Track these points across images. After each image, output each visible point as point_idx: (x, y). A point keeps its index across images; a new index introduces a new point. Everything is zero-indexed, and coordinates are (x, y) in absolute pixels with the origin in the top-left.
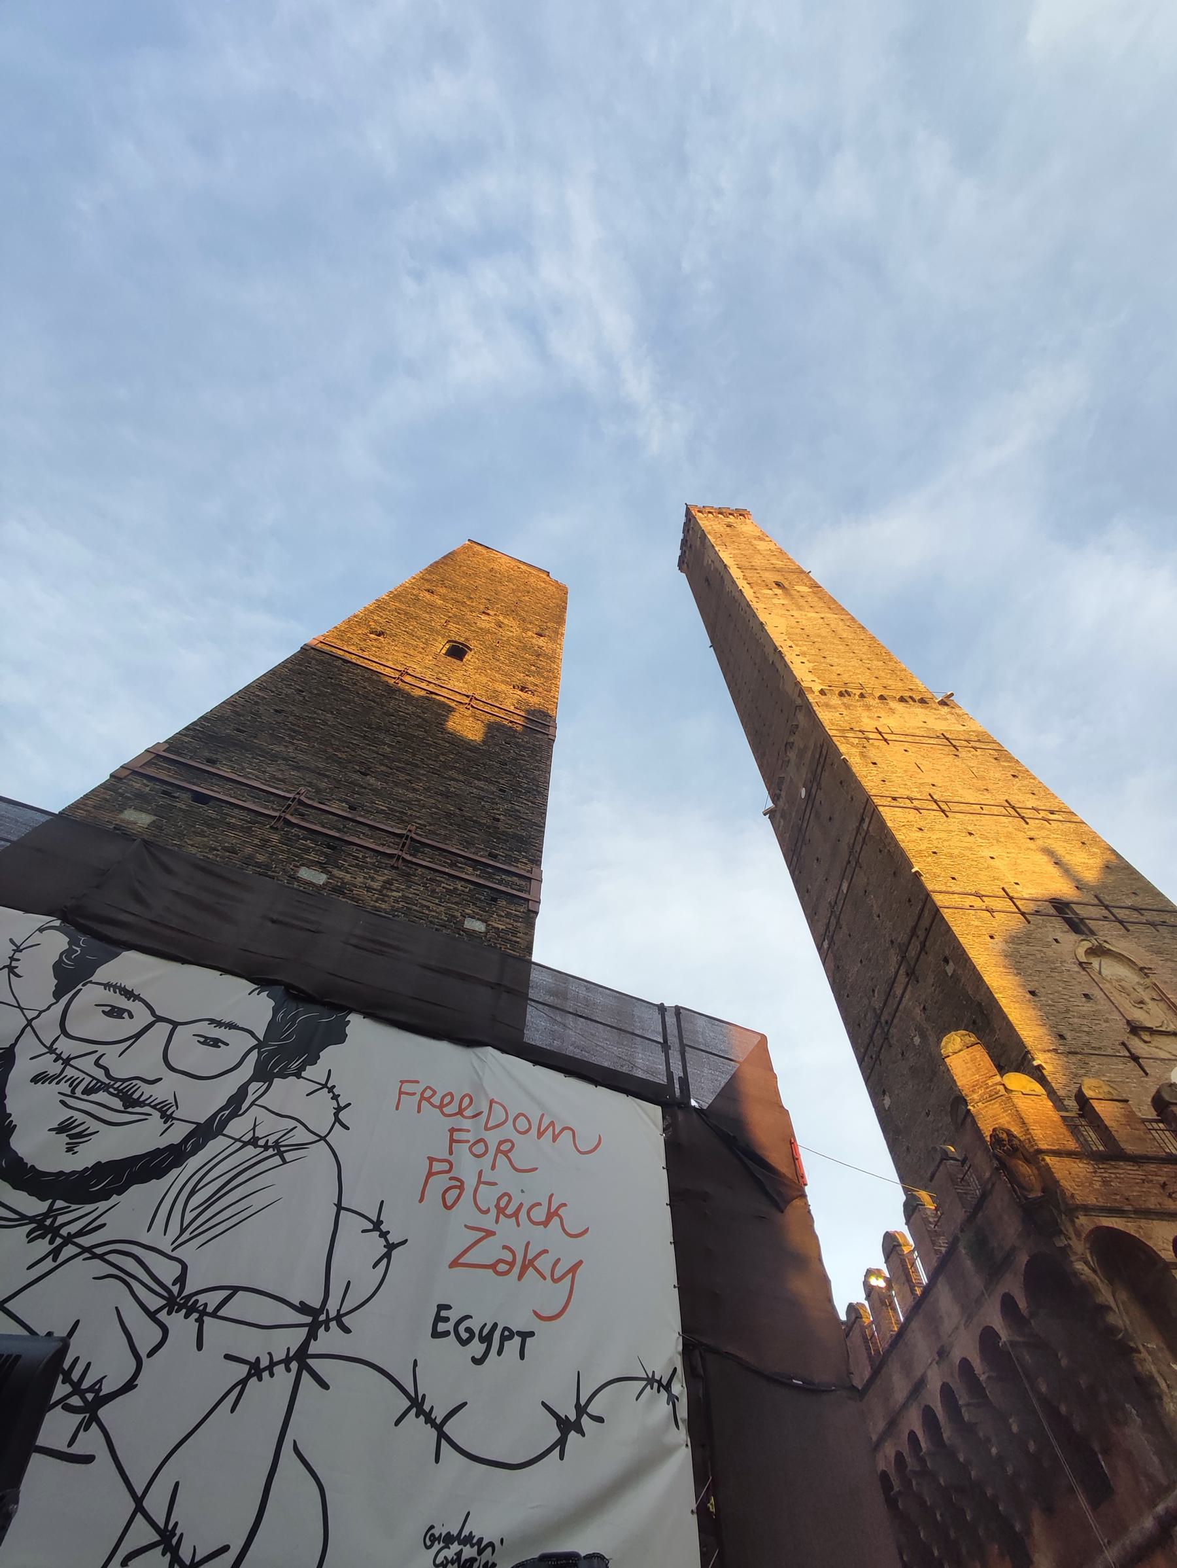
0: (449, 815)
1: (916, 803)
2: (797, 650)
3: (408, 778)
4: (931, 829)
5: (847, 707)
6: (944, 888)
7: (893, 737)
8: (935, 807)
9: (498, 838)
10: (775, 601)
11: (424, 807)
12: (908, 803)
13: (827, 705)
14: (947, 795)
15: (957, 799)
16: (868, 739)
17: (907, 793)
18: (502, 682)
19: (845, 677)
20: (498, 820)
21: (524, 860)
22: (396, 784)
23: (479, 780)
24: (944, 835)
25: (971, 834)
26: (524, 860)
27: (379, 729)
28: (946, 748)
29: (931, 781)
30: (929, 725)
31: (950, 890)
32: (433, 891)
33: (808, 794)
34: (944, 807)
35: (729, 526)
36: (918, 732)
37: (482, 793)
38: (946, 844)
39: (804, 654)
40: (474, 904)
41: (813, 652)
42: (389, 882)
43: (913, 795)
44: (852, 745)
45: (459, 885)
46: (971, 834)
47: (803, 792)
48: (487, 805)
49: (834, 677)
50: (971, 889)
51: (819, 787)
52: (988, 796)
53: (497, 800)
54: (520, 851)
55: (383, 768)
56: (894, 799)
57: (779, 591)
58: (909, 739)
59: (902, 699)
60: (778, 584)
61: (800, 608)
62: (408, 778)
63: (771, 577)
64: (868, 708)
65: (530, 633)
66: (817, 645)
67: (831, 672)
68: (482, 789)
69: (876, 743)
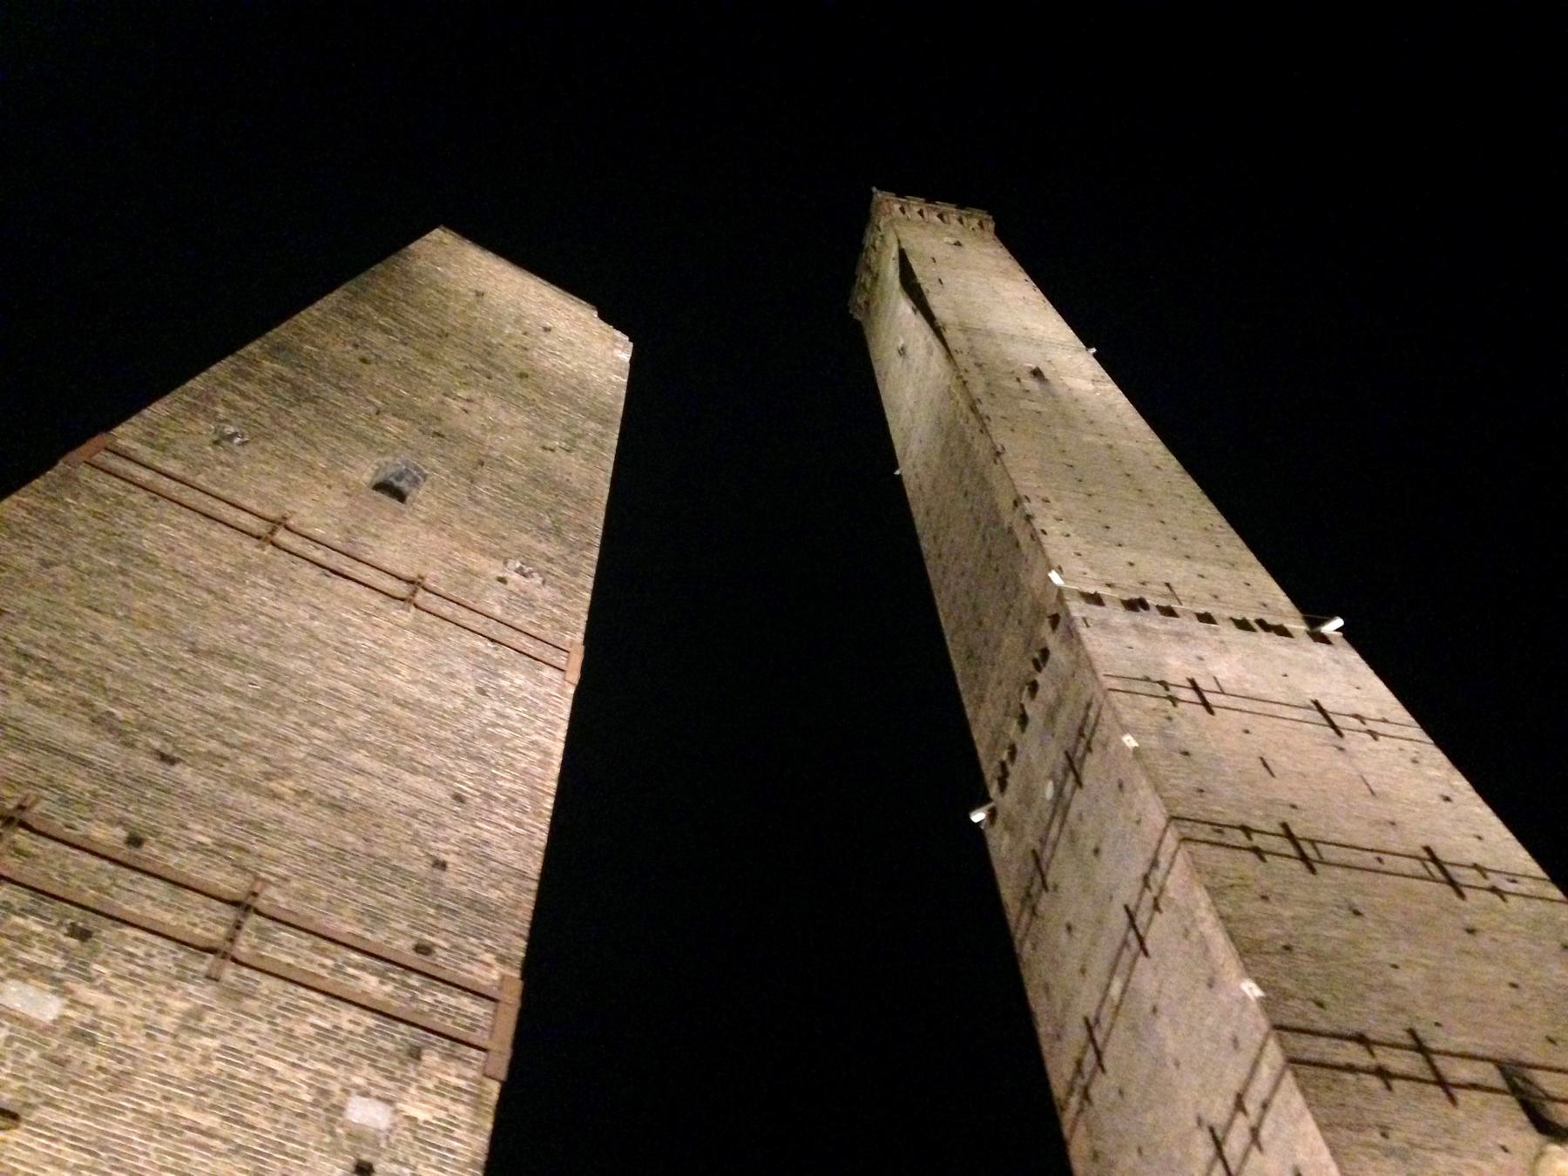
0: (341, 854)
1: (1257, 840)
3: (267, 768)
4: (1283, 898)
5: (1141, 630)
8: (1291, 850)
9: (439, 907)
11: (289, 835)
12: (1240, 838)
13: (1104, 625)
14: (1318, 830)
15: (1336, 837)
16: (1174, 700)
18: (483, 551)
20: (442, 865)
21: (488, 957)
22: (236, 782)
23: (414, 771)
24: (1304, 911)
25: (1357, 913)
26: (488, 957)
27: (211, 653)
32: (290, 1034)
33: (1059, 793)
34: (1309, 851)
37: (417, 804)
38: (1309, 930)
42: (197, 1014)
43: (1253, 823)
45: (346, 1017)
46: (1357, 913)
47: (1049, 791)
48: (425, 831)
50: (1354, 1027)
51: (1079, 782)
53: (446, 820)
55: (214, 745)
59: (1243, 625)
62: (267, 768)
68: (412, 792)
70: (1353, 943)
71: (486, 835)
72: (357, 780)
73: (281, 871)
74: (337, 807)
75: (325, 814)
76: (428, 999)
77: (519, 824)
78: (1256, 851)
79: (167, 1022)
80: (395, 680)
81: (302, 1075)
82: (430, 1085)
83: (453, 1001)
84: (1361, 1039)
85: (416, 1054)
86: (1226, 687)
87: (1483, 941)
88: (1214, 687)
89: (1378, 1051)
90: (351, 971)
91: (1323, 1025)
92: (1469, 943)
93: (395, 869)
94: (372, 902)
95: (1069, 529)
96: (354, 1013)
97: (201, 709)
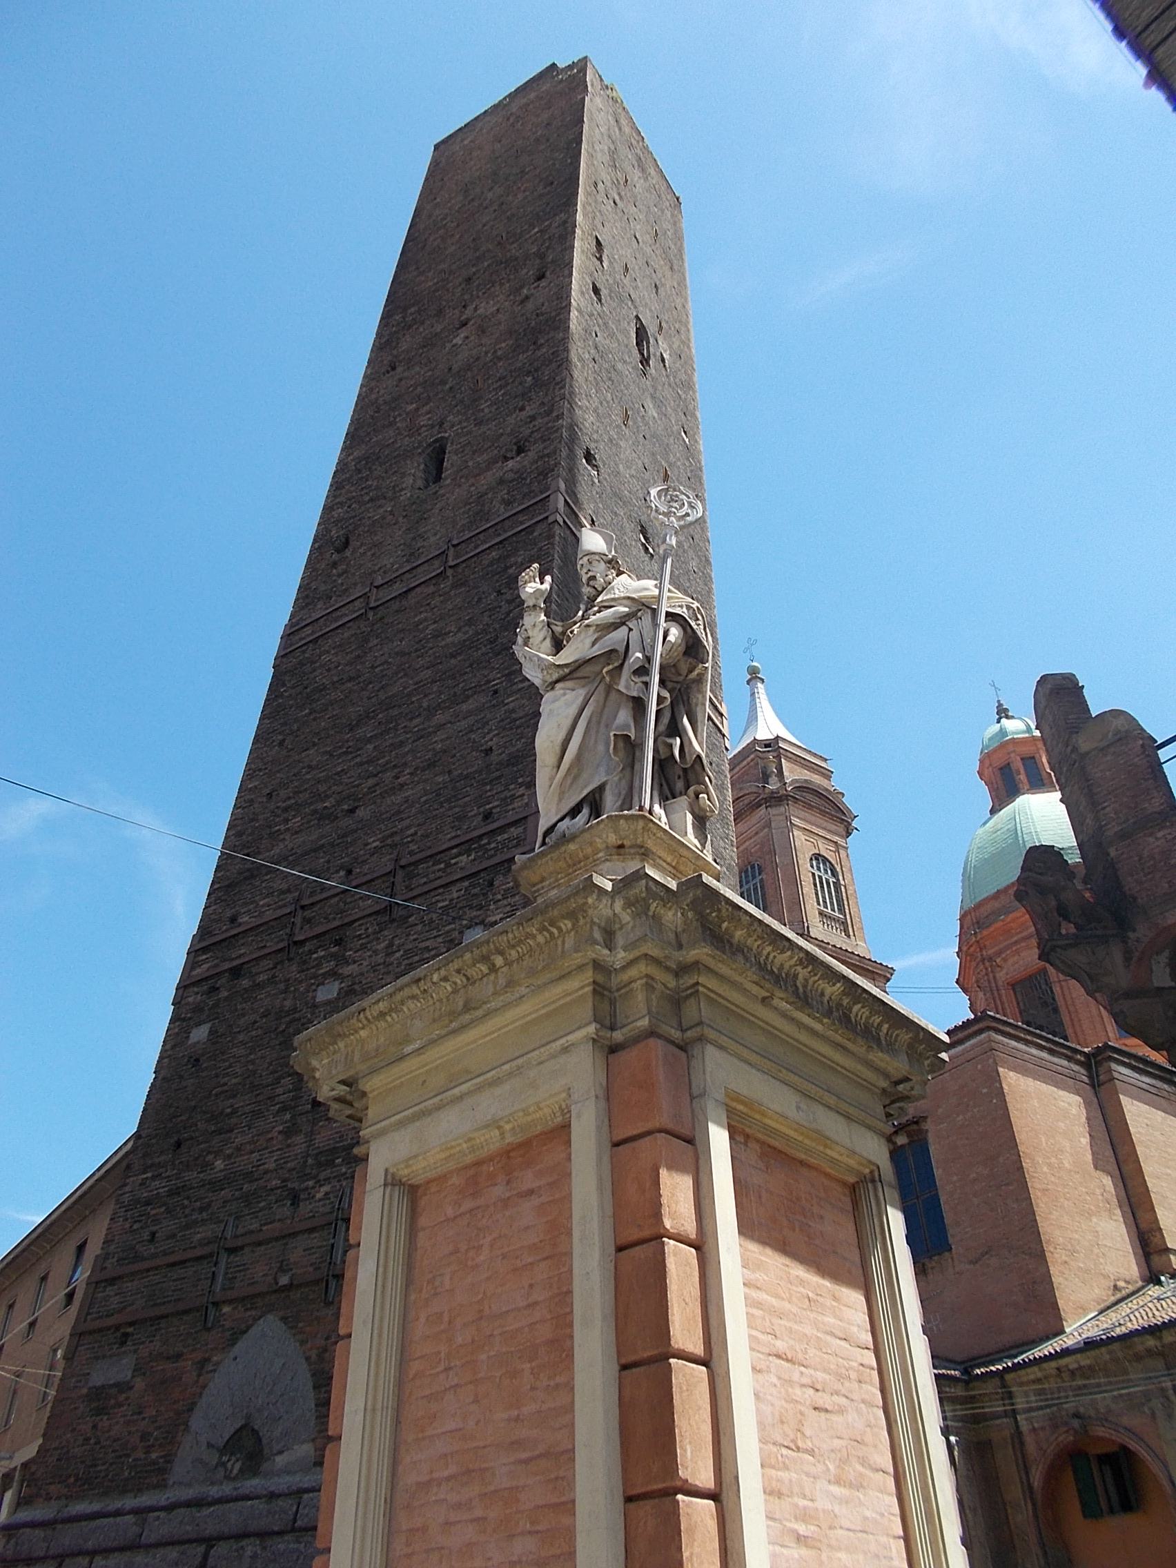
40: (471, 908)
42: (391, 945)
68: (470, 713)
72: (441, 735)
73: (412, 831)
74: (431, 765)
76: (493, 845)
79: (380, 958)
80: (449, 640)
81: (440, 940)
82: (499, 897)
83: (506, 836)
85: (491, 884)
90: (453, 861)
93: (467, 777)
94: (457, 810)
96: (458, 885)
97: (361, 764)
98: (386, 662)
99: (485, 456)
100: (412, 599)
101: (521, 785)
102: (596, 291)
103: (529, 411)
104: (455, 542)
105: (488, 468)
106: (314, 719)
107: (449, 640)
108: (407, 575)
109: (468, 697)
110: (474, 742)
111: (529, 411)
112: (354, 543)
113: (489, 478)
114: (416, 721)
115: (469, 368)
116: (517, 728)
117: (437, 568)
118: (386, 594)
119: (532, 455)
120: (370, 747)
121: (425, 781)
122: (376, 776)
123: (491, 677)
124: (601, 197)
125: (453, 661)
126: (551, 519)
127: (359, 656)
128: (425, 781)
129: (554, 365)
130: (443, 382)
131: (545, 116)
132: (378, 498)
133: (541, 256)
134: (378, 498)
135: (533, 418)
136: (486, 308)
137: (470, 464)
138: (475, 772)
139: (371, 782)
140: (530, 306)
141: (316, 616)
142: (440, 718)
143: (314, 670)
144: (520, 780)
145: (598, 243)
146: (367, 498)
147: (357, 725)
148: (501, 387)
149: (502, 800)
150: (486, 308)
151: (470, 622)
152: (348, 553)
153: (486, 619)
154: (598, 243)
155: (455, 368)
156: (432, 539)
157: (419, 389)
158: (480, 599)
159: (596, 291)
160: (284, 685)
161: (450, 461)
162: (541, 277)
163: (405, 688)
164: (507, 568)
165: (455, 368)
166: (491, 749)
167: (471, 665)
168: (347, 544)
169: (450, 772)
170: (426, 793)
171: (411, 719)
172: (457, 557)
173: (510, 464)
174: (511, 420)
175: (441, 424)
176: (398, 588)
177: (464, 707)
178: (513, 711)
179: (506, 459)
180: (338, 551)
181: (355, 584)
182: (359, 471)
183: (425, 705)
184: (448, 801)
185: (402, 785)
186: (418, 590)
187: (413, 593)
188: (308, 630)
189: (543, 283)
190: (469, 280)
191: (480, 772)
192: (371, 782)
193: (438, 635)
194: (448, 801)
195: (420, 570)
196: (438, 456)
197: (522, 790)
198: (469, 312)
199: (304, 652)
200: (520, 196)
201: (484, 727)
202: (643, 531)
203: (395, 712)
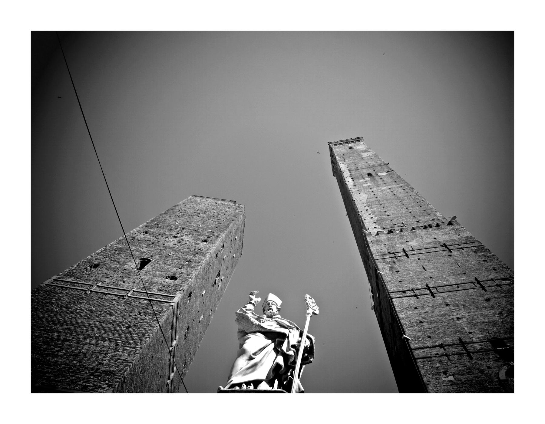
2: (370, 211)
4: (423, 307)
6: (421, 345)
7: (413, 252)
10: (365, 185)
12: (412, 293)
13: (378, 241)
15: (444, 283)
17: (411, 286)
19: (395, 222)
24: (427, 309)
25: (447, 305)
28: (445, 253)
29: (430, 275)
30: (438, 240)
31: (425, 345)
34: (434, 291)
35: (350, 148)
36: (429, 246)
38: (430, 315)
39: (373, 213)
41: (379, 210)
44: (387, 263)
46: (447, 305)
49: (389, 222)
52: (464, 277)
54: (104, 381)
56: (404, 292)
57: (368, 179)
58: (422, 251)
60: (369, 175)
61: (378, 185)
63: (365, 172)
64: (402, 237)
65: (198, 242)
66: (382, 206)
67: (387, 220)
69: (402, 258)
70: (444, 315)
71: (120, 353)
72: (86, 347)
75: (71, 358)
77: (133, 348)
78: (416, 296)
80: (112, 318)
84: (441, 346)
86: (415, 248)
87: (492, 302)
88: (411, 249)
89: (446, 348)
91: (429, 344)
92: (486, 304)
95: (373, 216)
98: (83, 310)
99: (160, 273)
100: (107, 297)
101: (106, 384)
102: (217, 256)
103: (182, 270)
104: (134, 290)
105: (159, 277)
106: (41, 312)
107: (112, 318)
108: (111, 289)
109: (106, 340)
110: (98, 357)
111: (182, 270)
112: (99, 268)
113: (157, 280)
114: (80, 336)
115: (170, 247)
116: (118, 362)
117: (123, 293)
118: (98, 290)
119: (176, 282)
120: (56, 334)
121: (69, 360)
122: (50, 346)
123: (119, 339)
124: (230, 236)
125: (108, 326)
126: (171, 304)
127: (75, 302)
128: (69, 360)
129: (197, 264)
130: (159, 246)
131: (227, 209)
132: (116, 261)
133: (209, 237)
134: (116, 261)
135: (182, 273)
136: (185, 238)
137: (154, 272)
138: (91, 368)
139: (46, 347)
140: (198, 246)
141: (68, 280)
142: (90, 341)
143: (54, 296)
144: (107, 382)
145: (223, 246)
146: (113, 259)
147: (56, 324)
148: (177, 259)
149: (95, 385)
150: (185, 238)
151: (123, 317)
152: (95, 270)
153: (130, 320)
154: (223, 246)
155: (166, 245)
156: (127, 284)
157: (150, 243)
158: (131, 312)
159: (217, 256)
160: (38, 294)
161: (148, 267)
162: (205, 241)
163: (84, 323)
164: (147, 309)
165: (166, 245)
166: (103, 364)
167: (114, 331)
168: (96, 266)
169: (81, 362)
170: (65, 364)
171: (79, 335)
172: (132, 294)
173: (167, 280)
174: (175, 269)
175: (152, 256)
176: (105, 291)
177: (102, 343)
178: (120, 355)
179: (166, 278)
180: (91, 267)
181: (90, 280)
182: (116, 251)
183: (88, 333)
184: (72, 372)
185: (58, 356)
186: (112, 296)
187: (109, 296)
188: (62, 283)
189: (205, 243)
190: (183, 228)
191: (93, 370)
192: (46, 347)
193: (108, 313)
194: (72, 372)
195: (116, 290)
196: (144, 263)
197: (105, 386)
198: (178, 235)
199: (55, 288)
200: (210, 221)
201: (105, 354)
202: (188, 329)
203: (75, 328)
